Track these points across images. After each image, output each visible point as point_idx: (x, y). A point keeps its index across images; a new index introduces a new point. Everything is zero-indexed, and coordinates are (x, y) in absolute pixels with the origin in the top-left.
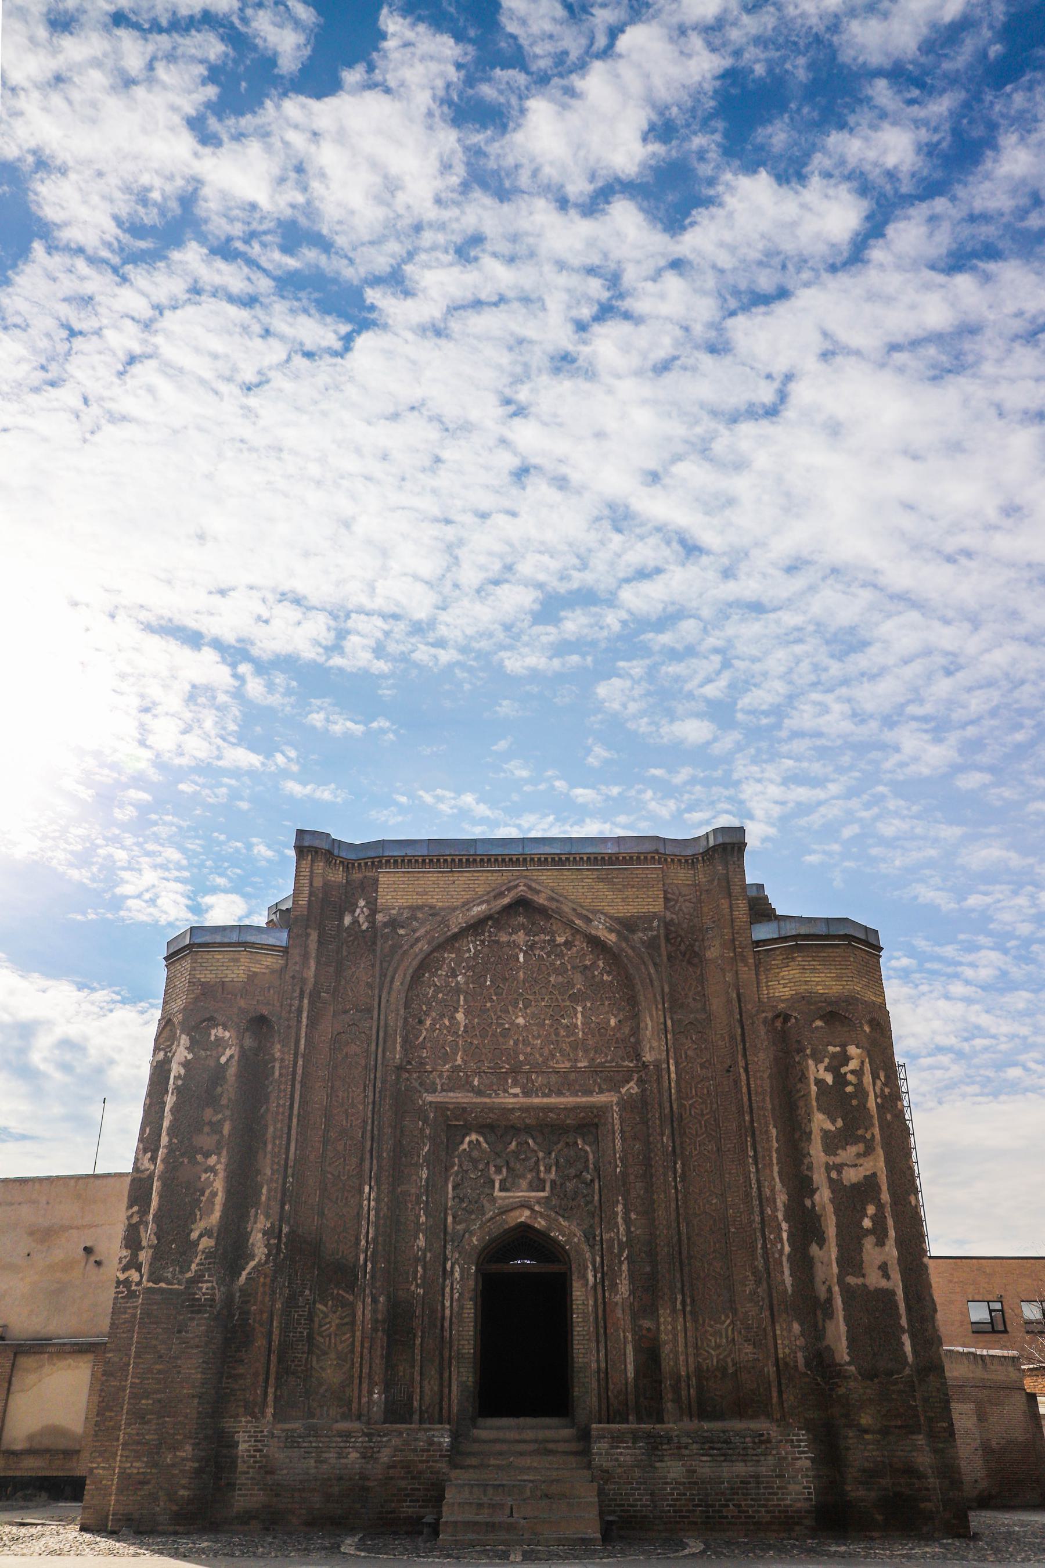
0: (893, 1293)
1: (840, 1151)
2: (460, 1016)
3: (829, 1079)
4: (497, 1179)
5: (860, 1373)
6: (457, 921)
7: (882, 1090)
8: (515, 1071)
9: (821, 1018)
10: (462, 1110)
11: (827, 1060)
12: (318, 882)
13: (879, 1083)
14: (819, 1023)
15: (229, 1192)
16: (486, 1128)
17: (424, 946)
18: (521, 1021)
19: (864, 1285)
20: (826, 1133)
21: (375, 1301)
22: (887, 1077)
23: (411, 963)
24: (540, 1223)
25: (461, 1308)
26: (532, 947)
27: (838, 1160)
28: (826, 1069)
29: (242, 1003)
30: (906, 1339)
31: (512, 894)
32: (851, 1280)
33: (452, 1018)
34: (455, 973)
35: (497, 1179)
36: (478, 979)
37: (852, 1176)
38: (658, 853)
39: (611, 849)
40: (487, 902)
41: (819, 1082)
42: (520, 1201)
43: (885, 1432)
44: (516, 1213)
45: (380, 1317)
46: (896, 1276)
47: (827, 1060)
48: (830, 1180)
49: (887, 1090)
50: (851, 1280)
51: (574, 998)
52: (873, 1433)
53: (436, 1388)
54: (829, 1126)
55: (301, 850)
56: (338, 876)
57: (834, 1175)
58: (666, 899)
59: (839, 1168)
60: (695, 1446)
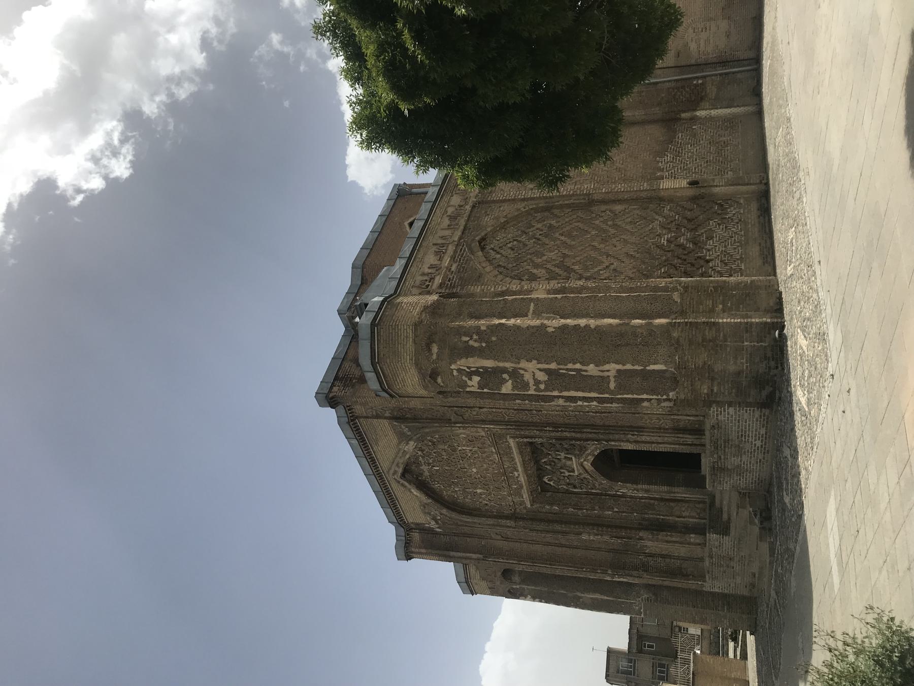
0: (618, 371)
1: (525, 379)
2: (479, 491)
3: (476, 379)
4: (567, 474)
5: (674, 390)
6: (424, 499)
7: (475, 341)
8: (505, 474)
9: (435, 380)
10: (532, 492)
11: (464, 378)
12: (423, 551)
13: (471, 343)
14: (439, 380)
15: (595, 592)
16: (540, 478)
17: (444, 511)
18: (474, 470)
19: (615, 377)
20: (514, 388)
21: (641, 539)
22: (466, 335)
23: (454, 515)
24: (591, 458)
25: (642, 490)
26: (429, 464)
27: (532, 382)
28: (470, 379)
29: (498, 583)
30: (652, 367)
31: (402, 481)
32: (612, 385)
33: (481, 494)
34: (455, 492)
35: (567, 474)
36: (456, 484)
37: (542, 377)
38: (348, 423)
39: (355, 442)
40: (409, 490)
41: (481, 386)
42: (580, 465)
43: (713, 379)
44: (587, 467)
45: (650, 537)
46: (607, 367)
47: (464, 378)
48: (546, 389)
49: (475, 337)
50: (612, 385)
51: (454, 450)
52: (712, 385)
53: (687, 505)
54: (509, 384)
55: (409, 558)
56: (416, 536)
57: (542, 386)
58: (377, 417)
59: (537, 382)
60: (720, 453)
